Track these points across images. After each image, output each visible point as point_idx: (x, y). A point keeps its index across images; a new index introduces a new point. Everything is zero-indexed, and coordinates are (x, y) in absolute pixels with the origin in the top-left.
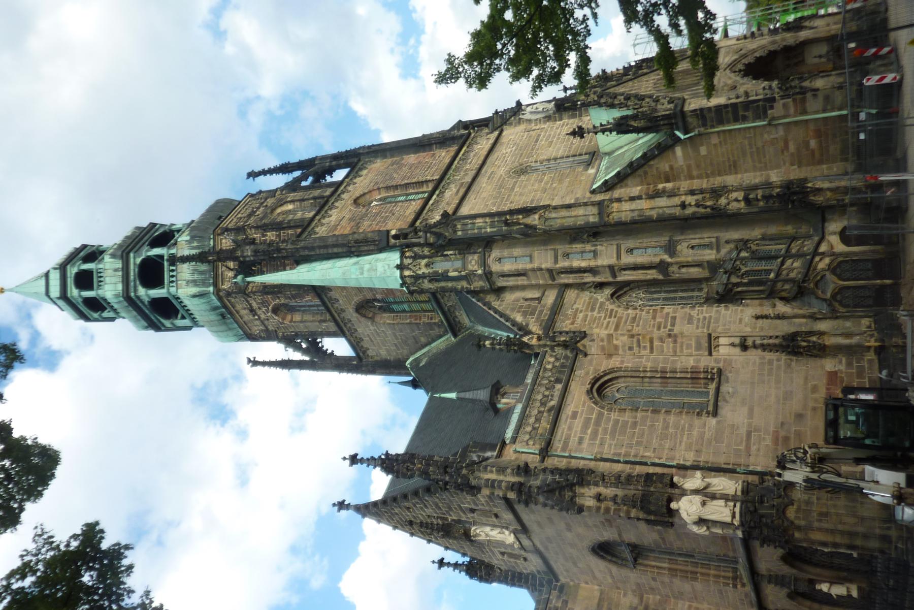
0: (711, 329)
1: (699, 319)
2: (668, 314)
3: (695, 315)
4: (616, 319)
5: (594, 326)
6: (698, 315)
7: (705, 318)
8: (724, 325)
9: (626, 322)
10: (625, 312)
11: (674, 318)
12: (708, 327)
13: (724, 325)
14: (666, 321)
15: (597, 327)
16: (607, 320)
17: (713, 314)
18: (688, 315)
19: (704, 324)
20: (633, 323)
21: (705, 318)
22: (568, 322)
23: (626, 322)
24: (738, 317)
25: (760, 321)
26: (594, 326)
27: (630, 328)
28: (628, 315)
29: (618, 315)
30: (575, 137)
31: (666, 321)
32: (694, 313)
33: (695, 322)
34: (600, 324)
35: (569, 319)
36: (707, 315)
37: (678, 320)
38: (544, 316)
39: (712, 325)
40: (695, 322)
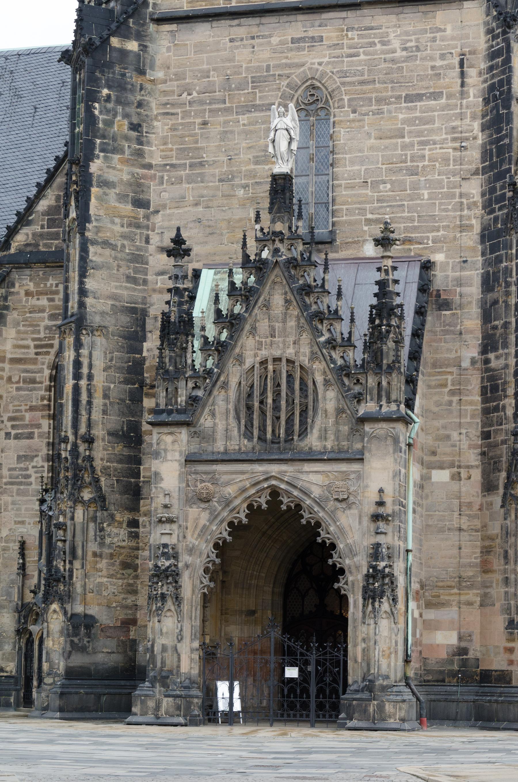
0: (8, 487)
1: (27, 469)
2: (39, 426)
3: (34, 464)
4: (33, 356)
5: (21, 328)
6: (33, 467)
7: (29, 476)
8: (13, 503)
9: (27, 371)
10: (45, 367)
11: (30, 436)
12: (12, 483)
13: (13, 503)
14: (26, 426)
15: (18, 332)
16: (32, 344)
17: (34, 486)
18: (34, 454)
19: (17, 477)
20: (25, 381)
21: (29, 476)
22: (31, 286)
23: (27, 371)
24: (27, 519)
25: (16, 546)
26: (21, 328)
27: (15, 379)
28: (41, 371)
29: (39, 357)
30: (173, 240)
31: (26, 426)
32: (39, 461)
33: (22, 465)
34: (22, 336)
35: (37, 285)
36: (32, 479)
37: (25, 442)
38: (45, 245)
39: (15, 487)
40: (22, 465)
